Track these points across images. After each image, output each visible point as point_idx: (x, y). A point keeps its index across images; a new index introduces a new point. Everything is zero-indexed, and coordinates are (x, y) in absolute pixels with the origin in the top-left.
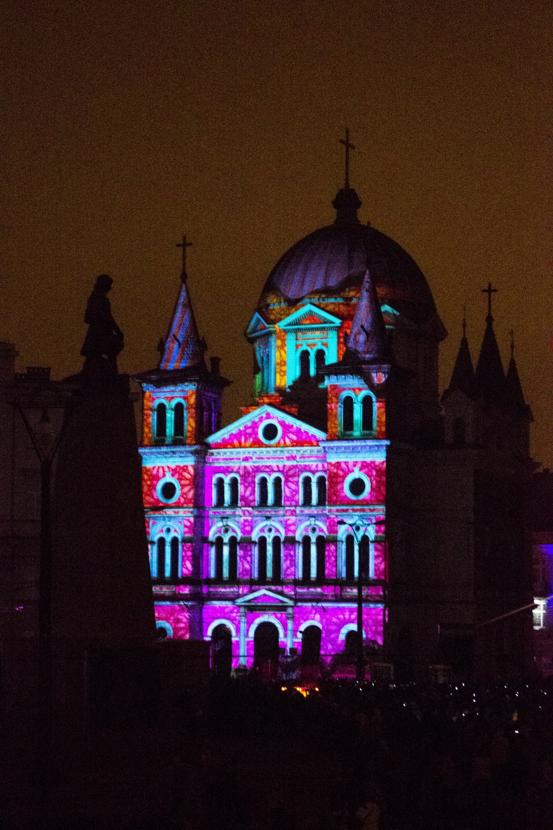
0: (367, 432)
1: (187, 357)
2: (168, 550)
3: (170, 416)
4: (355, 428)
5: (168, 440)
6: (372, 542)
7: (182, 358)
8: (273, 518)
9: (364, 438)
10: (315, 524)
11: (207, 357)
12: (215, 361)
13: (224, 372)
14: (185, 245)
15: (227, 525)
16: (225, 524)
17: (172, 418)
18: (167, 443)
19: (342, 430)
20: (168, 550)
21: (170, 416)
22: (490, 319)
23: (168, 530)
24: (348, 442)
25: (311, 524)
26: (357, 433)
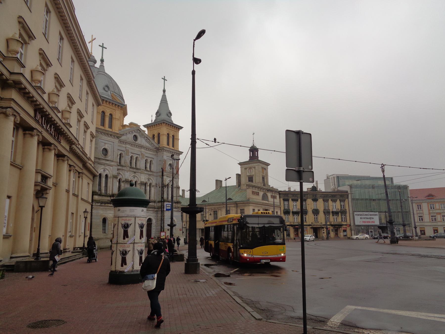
2: (103, 180)
6: (175, 187)
8: (136, 173)
10: (150, 178)
15: (120, 173)
20: (103, 180)
23: (104, 170)
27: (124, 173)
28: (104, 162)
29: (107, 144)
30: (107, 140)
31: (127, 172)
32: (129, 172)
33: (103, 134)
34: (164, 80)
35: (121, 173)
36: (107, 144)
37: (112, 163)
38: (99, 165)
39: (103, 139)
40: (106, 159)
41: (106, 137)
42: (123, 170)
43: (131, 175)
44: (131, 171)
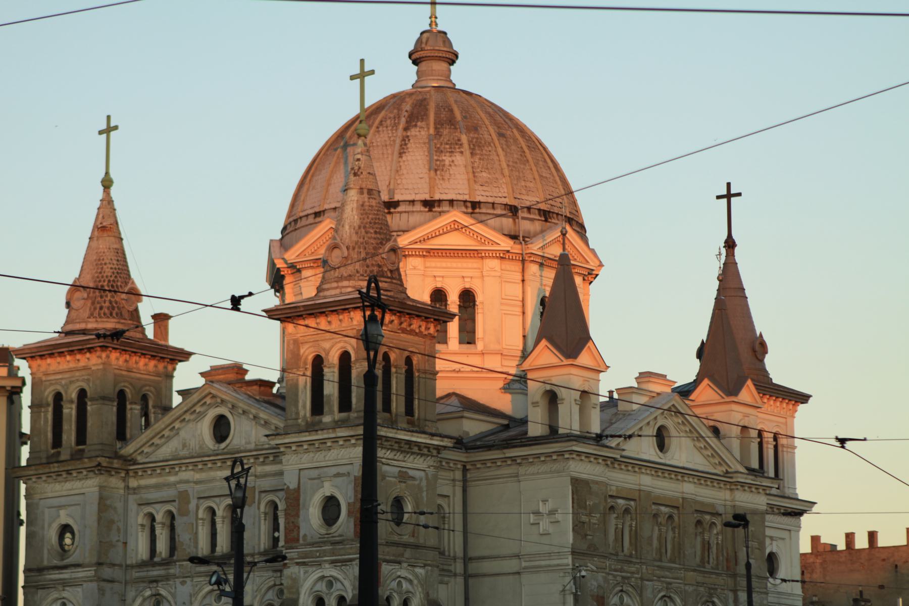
0: (344, 415)
1: (99, 314)
3: (70, 411)
4: (326, 409)
5: (65, 455)
7: (91, 315)
9: (338, 424)
11: (146, 311)
12: (161, 319)
13: (175, 340)
14: (109, 130)
15: (159, 595)
16: (154, 592)
17: (71, 415)
18: (62, 458)
19: (308, 414)
21: (70, 411)
22: (730, 244)
24: (310, 435)
25: (275, 585)
26: (327, 419)
27: (173, 591)
28: (53, 577)
29: (60, 507)
30: (65, 493)
31: (183, 583)
32: (188, 580)
33: (44, 478)
34: (366, 78)
35: (163, 592)
36: (60, 507)
37: (80, 573)
38: (40, 592)
39: (50, 495)
40: (66, 562)
41: (57, 487)
42: (167, 578)
43: (200, 590)
44: (199, 574)
